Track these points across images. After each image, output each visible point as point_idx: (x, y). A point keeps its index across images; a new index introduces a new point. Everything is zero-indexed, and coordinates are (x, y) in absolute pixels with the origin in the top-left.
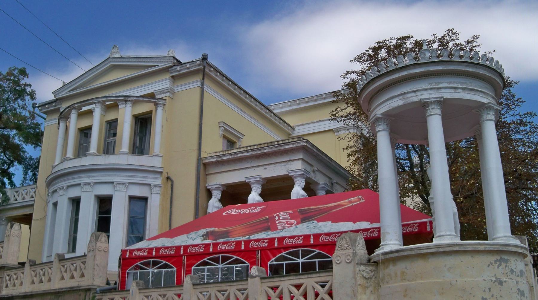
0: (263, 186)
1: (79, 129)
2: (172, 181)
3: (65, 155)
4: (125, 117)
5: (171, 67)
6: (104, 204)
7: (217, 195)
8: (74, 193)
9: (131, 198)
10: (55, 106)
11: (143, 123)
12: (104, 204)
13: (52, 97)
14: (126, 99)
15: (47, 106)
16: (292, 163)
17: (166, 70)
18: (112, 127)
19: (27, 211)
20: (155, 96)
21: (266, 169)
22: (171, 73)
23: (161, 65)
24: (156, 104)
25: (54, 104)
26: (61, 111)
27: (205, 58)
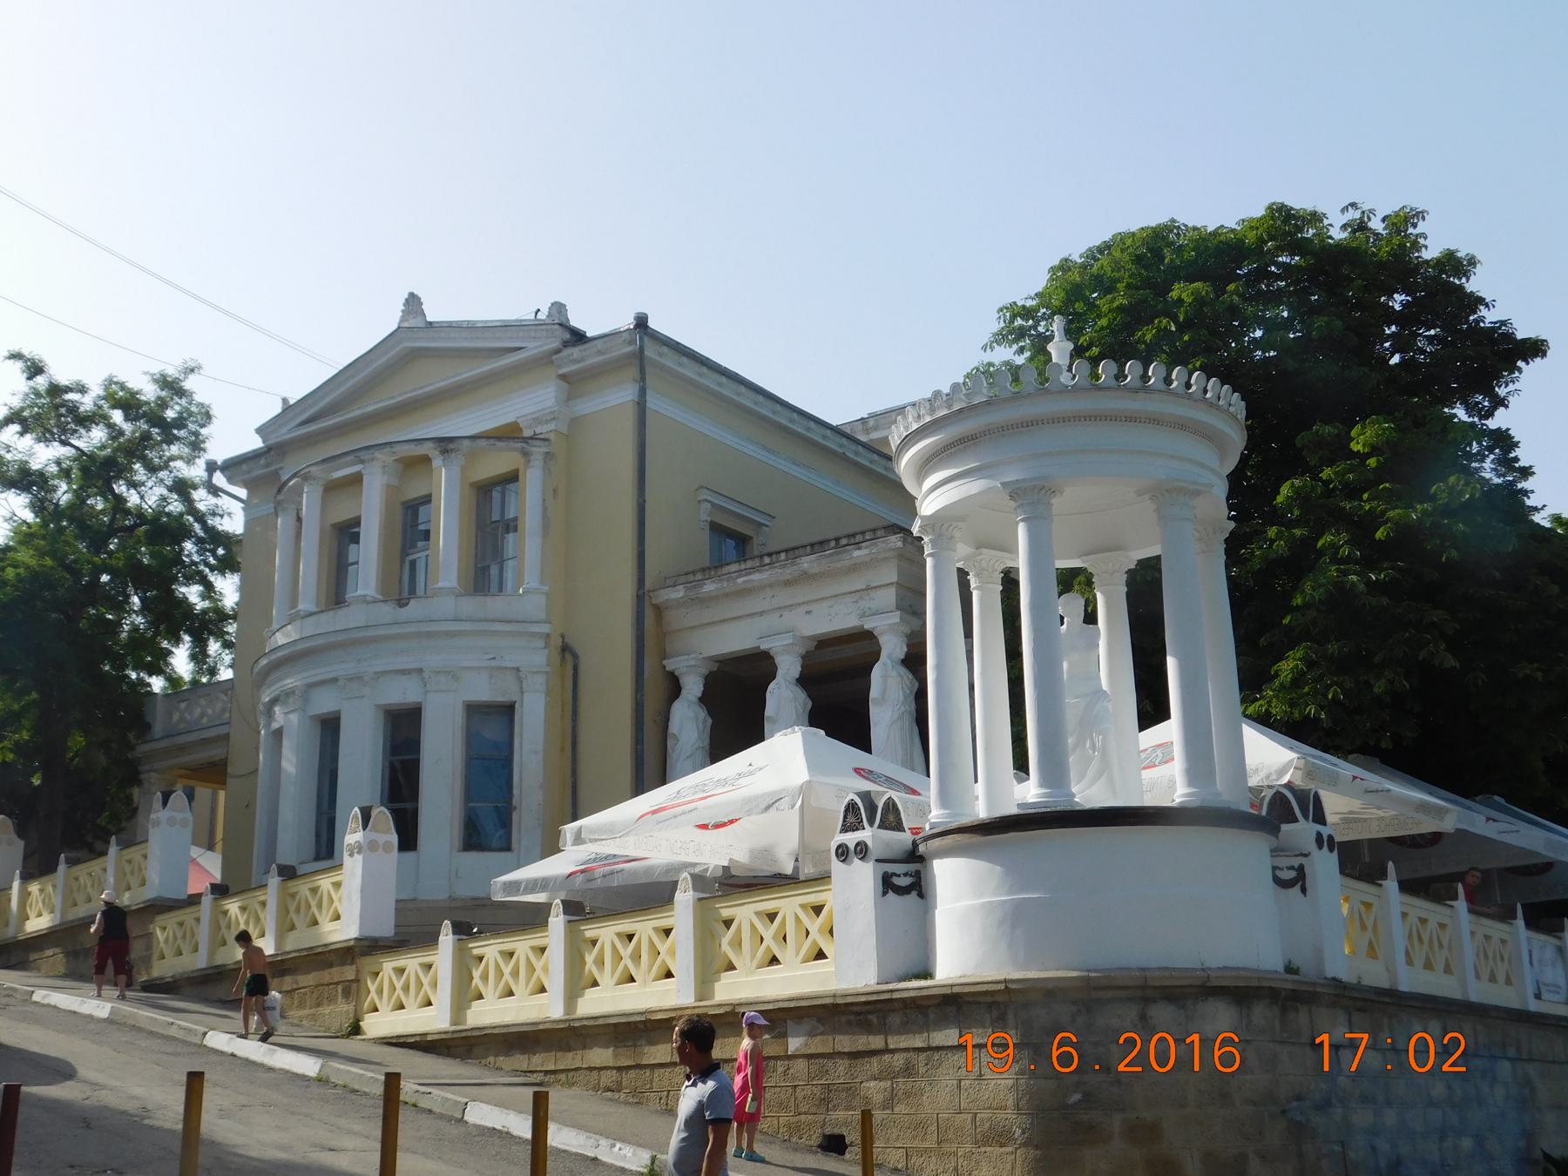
0: (806, 658)
1: (334, 526)
2: (575, 656)
3: (294, 602)
4: (446, 491)
5: (558, 351)
6: (403, 728)
7: (693, 687)
8: (325, 703)
9: (475, 711)
10: (268, 465)
11: (490, 507)
12: (403, 728)
13: (257, 443)
14: (445, 444)
15: (244, 467)
16: (872, 594)
17: (547, 359)
18: (411, 526)
19: (215, 753)
20: (521, 430)
21: (808, 612)
22: (559, 367)
23: (534, 347)
24: (526, 454)
25: (262, 461)
26: (285, 478)
27: (641, 322)
